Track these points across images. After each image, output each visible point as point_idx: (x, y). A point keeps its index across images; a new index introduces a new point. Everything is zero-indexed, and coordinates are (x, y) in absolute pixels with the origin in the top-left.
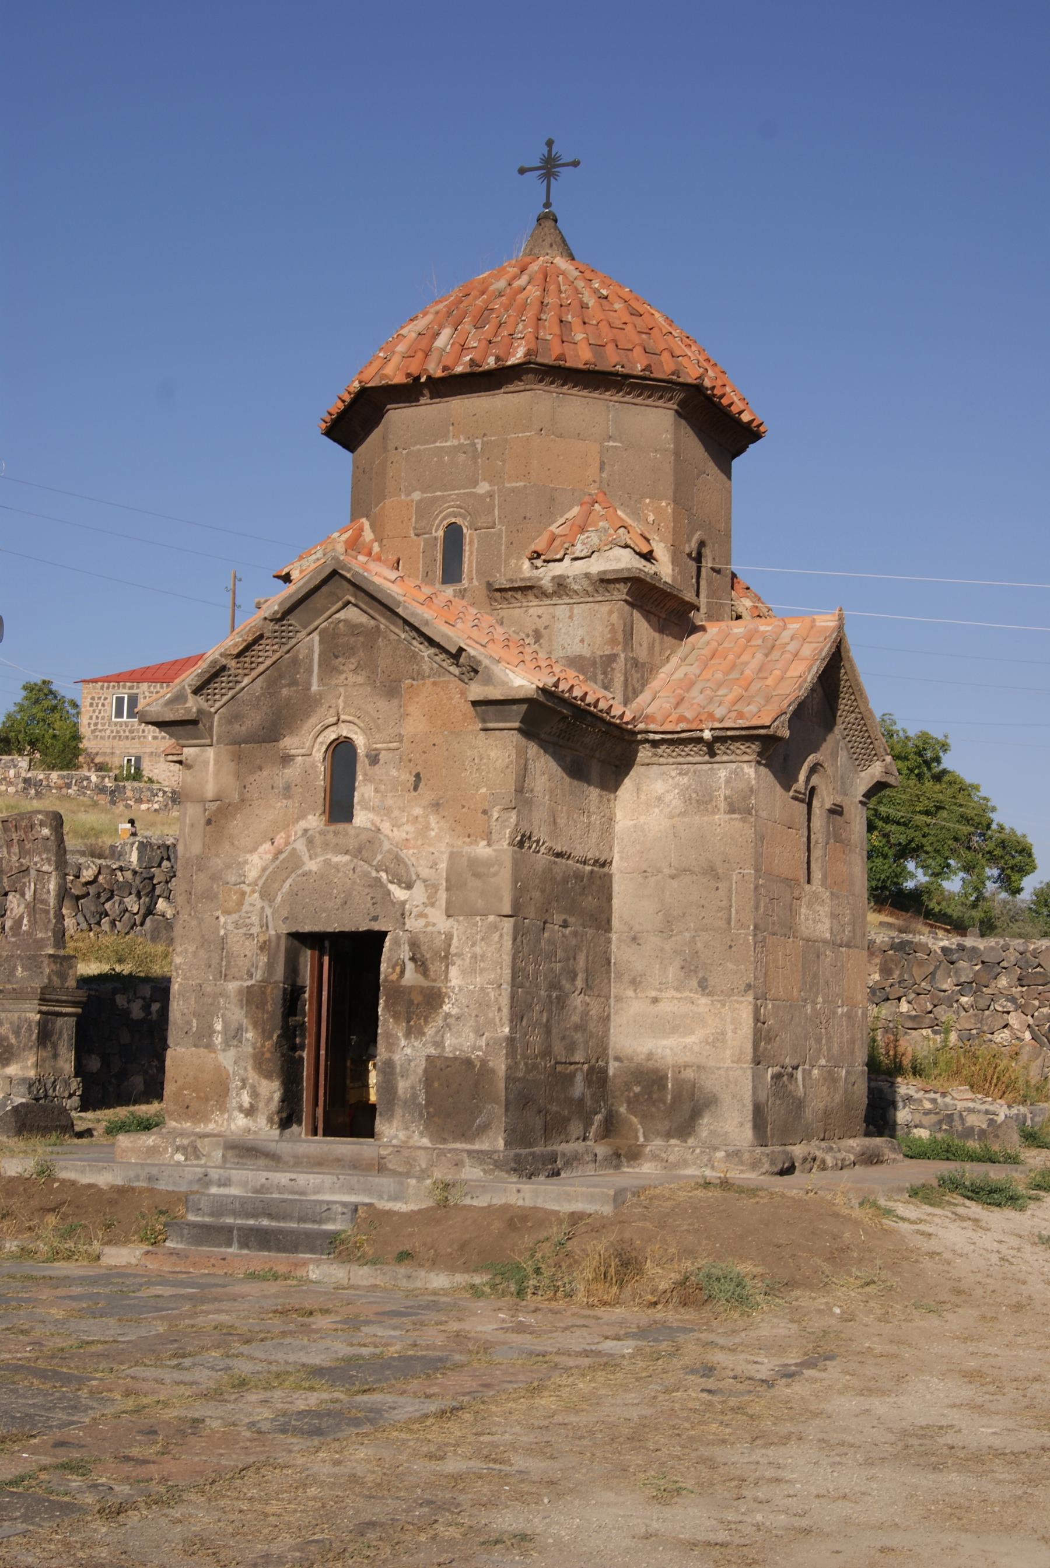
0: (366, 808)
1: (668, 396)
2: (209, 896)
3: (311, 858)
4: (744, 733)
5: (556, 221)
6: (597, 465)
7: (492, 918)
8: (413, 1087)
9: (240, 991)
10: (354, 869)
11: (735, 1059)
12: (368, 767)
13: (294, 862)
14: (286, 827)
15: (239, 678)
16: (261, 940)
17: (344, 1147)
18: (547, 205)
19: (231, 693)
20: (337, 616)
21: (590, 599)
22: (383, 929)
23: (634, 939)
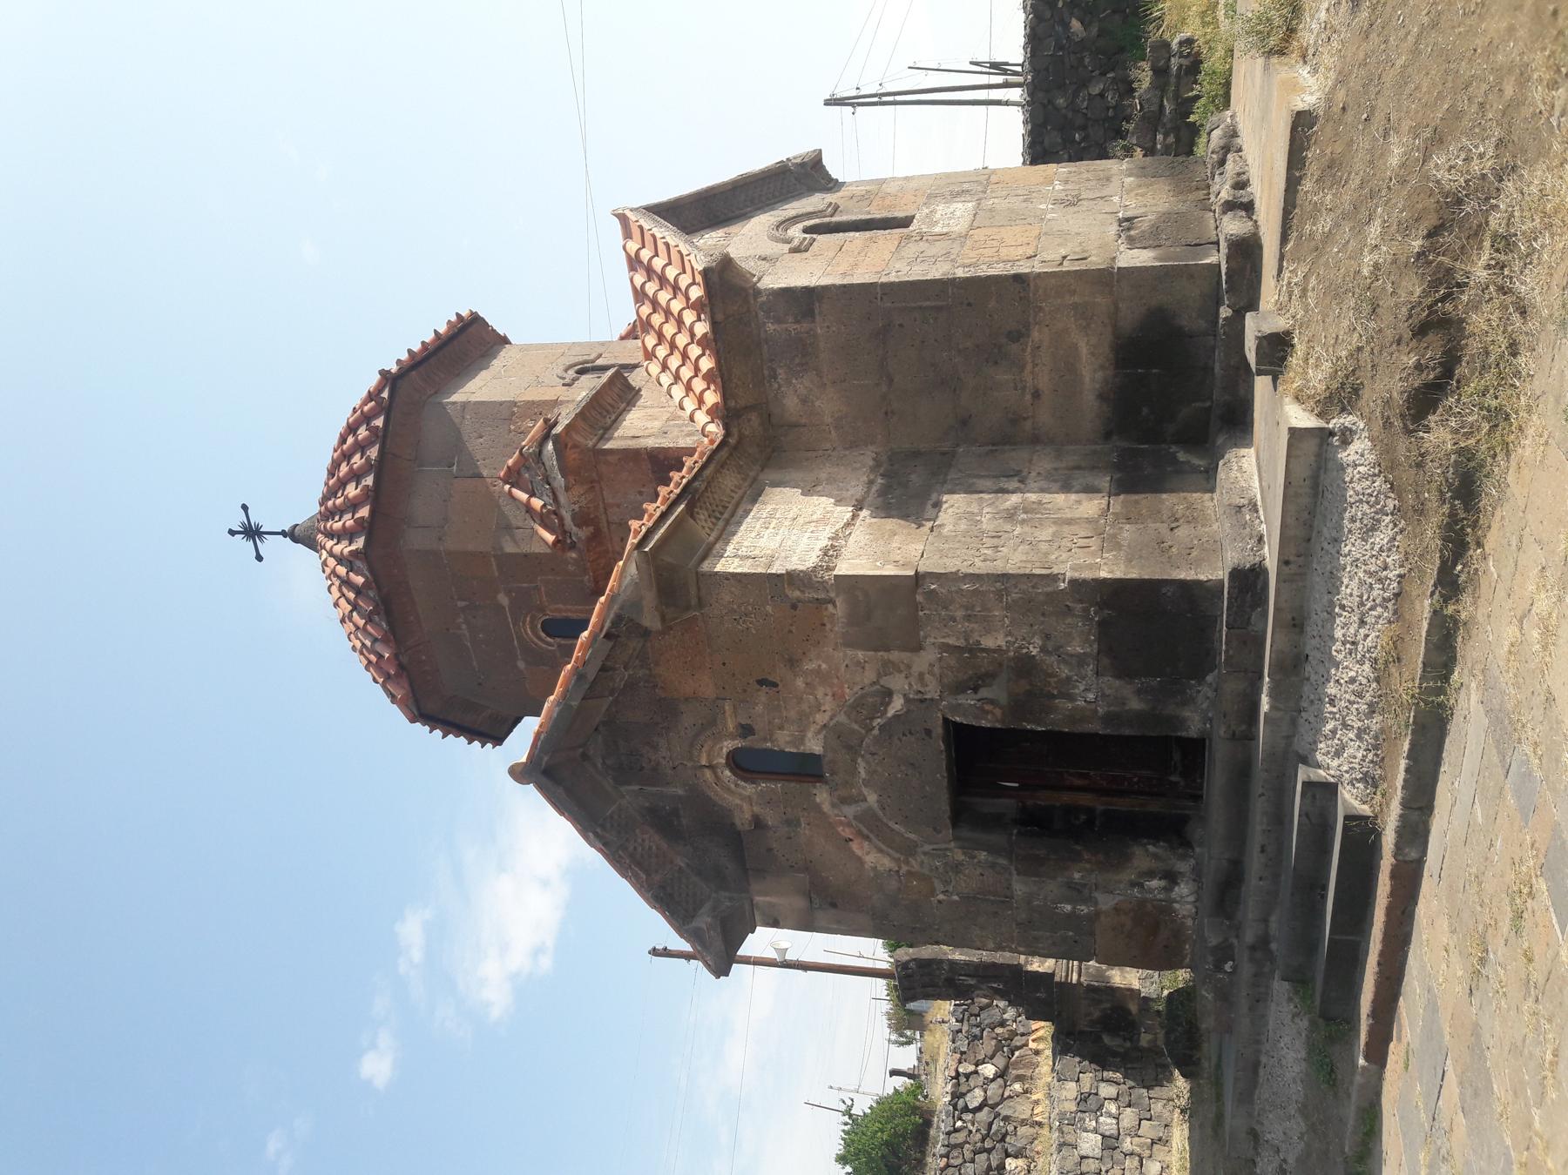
5: (298, 525)
7: (919, 598)
8: (1139, 692)
10: (873, 754)
12: (756, 736)
15: (677, 868)
16: (963, 857)
17: (1217, 780)
18: (284, 534)
20: (599, 765)
22: (940, 722)
23: (965, 423)
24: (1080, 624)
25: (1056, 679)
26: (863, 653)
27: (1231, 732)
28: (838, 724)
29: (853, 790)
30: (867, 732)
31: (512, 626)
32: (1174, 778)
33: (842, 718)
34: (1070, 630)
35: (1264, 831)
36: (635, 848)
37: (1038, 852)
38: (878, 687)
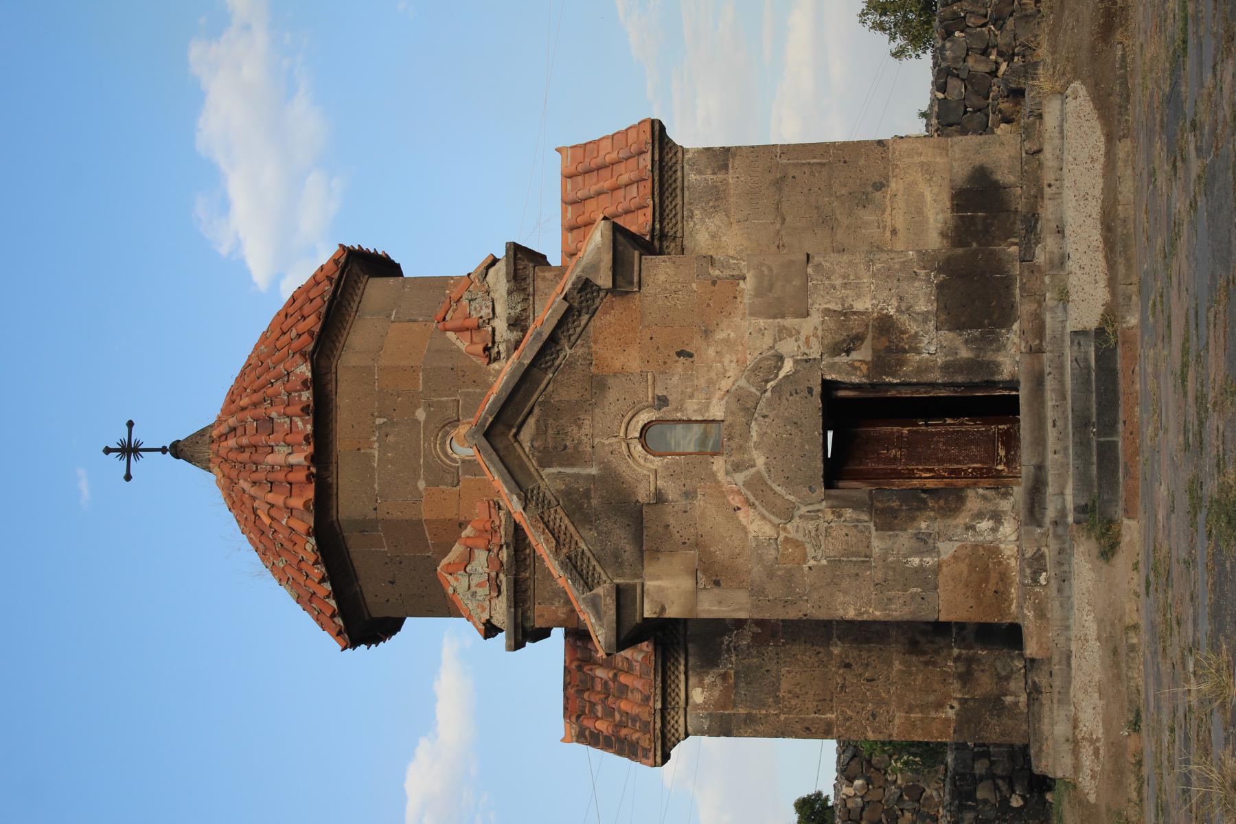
0: (707, 407)
4: (657, 146)
6: (411, 324)
7: (810, 270)
8: (966, 342)
9: (882, 539)
10: (765, 417)
13: (757, 484)
14: (723, 495)
15: (580, 550)
18: (164, 450)
19: (594, 562)
20: (527, 450)
21: (531, 298)
22: (820, 381)
25: (907, 336)
26: (765, 320)
28: (740, 388)
31: (422, 442)
32: (1000, 467)
33: (742, 382)
35: (1054, 406)
36: (549, 521)
38: (773, 351)
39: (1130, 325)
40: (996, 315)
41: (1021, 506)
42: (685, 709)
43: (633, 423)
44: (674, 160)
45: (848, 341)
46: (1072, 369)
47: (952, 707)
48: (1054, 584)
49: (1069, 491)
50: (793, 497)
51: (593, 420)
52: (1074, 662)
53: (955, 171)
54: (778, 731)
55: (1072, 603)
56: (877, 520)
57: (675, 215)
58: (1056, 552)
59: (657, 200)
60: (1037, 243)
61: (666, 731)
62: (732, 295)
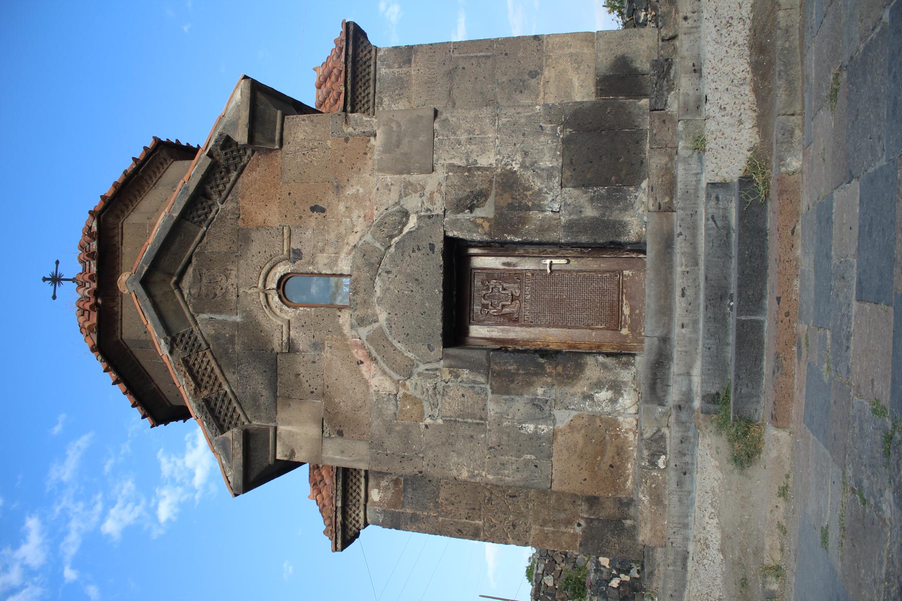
0: (334, 262)
1: (162, 160)
2: (406, 435)
3: (376, 321)
4: (351, 43)
7: (436, 126)
8: (592, 200)
9: (497, 402)
10: (386, 272)
11: (591, 44)
13: (379, 339)
14: (347, 348)
15: (222, 392)
19: (235, 404)
20: (186, 296)
22: (442, 238)
24: (549, 142)
25: (531, 192)
27: (657, 204)
28: (366, 243)
29: (369, 311)
30: (386, 250)
33: (368, 238)
34: (542, 147)
35: (683, 273)
36: (194, 364)
37: (509, 368)
38: (398, 207)
39: (791, 169)
40: (624, 172)
41: (641, 377)
42: (365, 506)
43: (271, 274)
44: (368, 57)
45: (472, 198)
46: (707, 229)
47: (579, 525)
48: (672, 477)
49: (696, 371)
50: (411, 354)
51: (238, 271)
52: (690, 564)
53: (599, 60)
54: (436, 530)
55: (693, 499)
56: (494, 383)
57: (368, 102)
58: (677, 441)
59: (349, 87)
60: (670, 89)
61: (347, 523)
62: (363, 151)
